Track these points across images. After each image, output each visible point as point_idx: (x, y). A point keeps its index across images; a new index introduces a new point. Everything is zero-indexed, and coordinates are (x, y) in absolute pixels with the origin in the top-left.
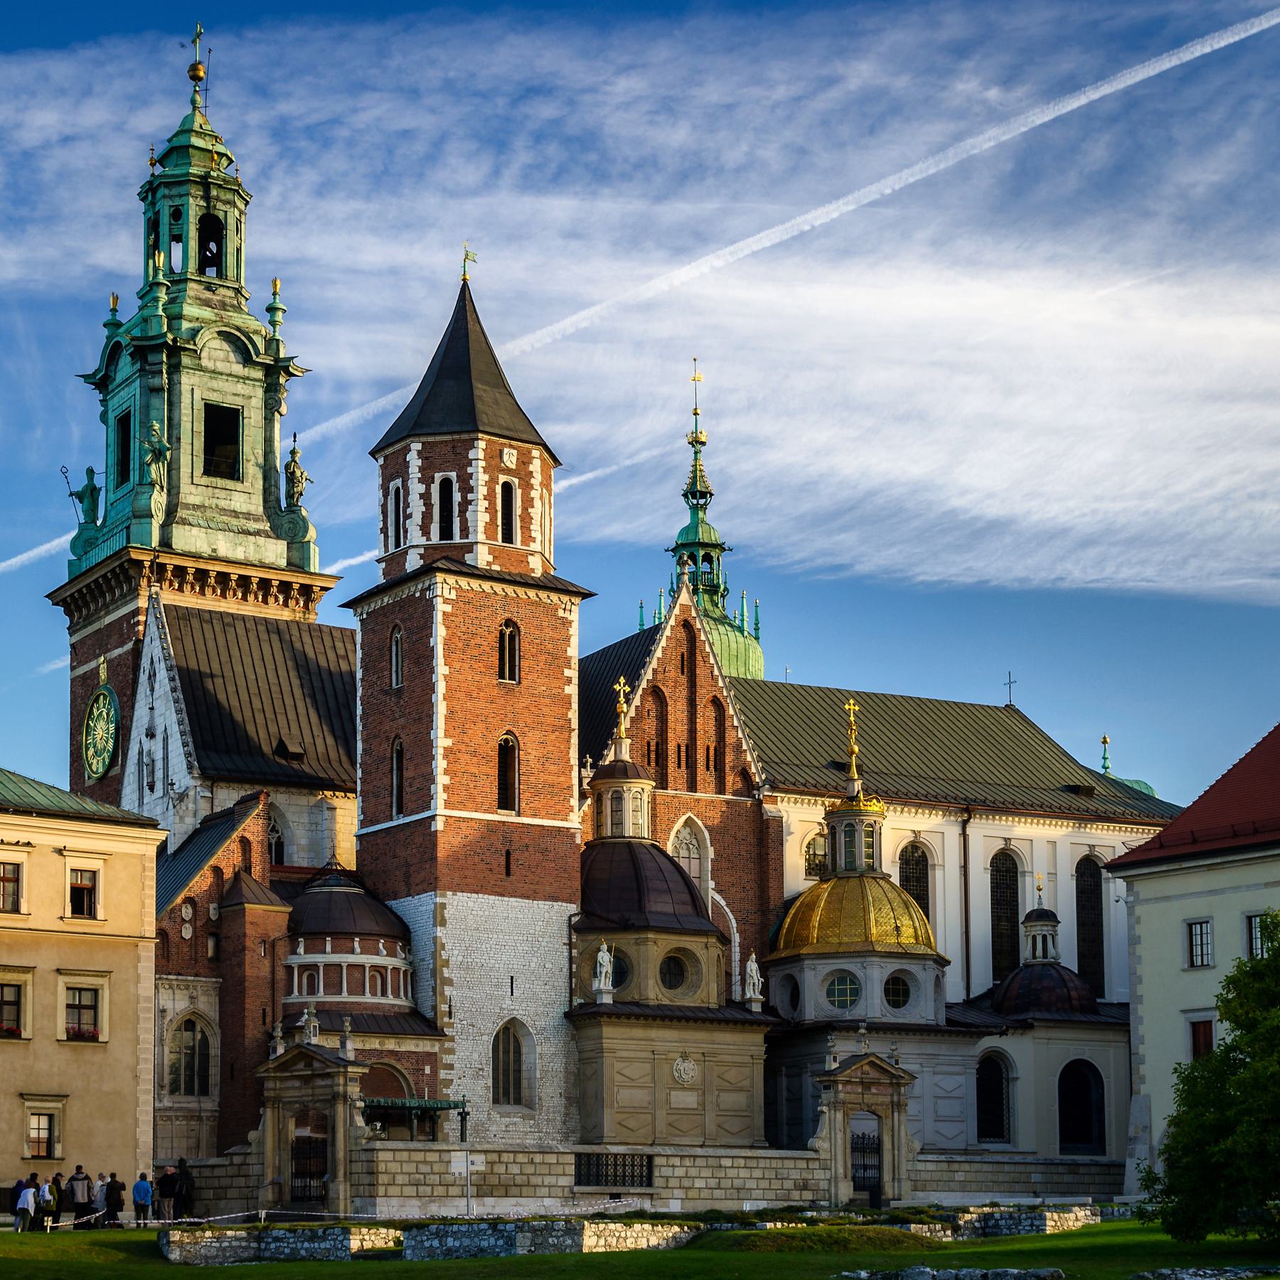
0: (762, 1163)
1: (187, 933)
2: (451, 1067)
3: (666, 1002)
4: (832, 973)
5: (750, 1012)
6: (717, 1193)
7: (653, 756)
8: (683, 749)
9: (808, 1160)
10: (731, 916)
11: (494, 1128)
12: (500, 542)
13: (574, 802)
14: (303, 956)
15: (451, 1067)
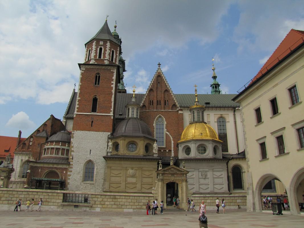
0: (131, 198)
1: (31, 144)
2: (71, 171)
3: (127, 154)
4: (185, 147)
5: (154, 156)
6: (114, 206)
7: (151, 103)
8: (159, 101)
9: (149, 197)
10: (171, 137)
11: (82, 187)
12: (98, 58)
13: (112, 110)
14: (46, 147)
15: (71, 171)
